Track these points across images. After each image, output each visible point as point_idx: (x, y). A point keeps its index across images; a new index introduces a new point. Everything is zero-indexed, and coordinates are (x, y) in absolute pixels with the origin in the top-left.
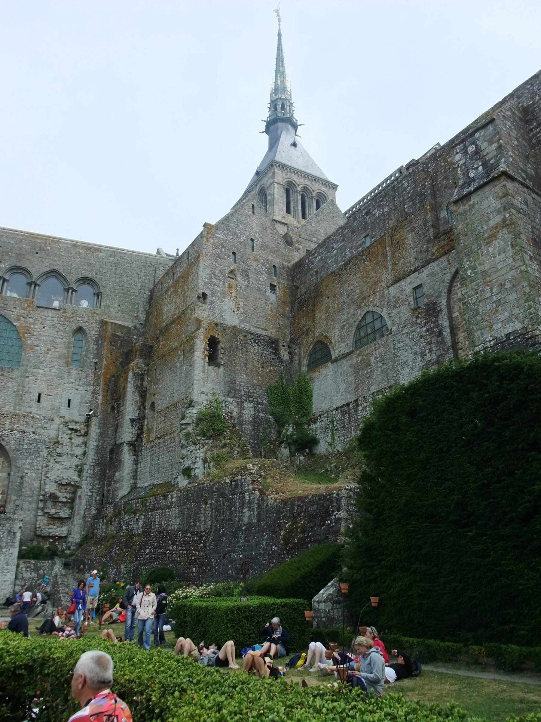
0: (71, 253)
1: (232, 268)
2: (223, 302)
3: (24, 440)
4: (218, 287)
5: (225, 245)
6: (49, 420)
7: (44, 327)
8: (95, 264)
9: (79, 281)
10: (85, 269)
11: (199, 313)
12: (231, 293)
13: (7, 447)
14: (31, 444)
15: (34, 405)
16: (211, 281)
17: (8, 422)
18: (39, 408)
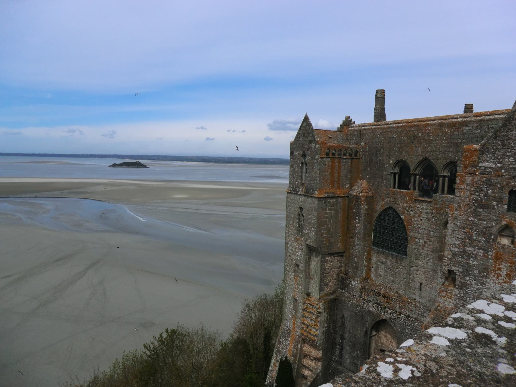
0: (439, 135)
1: (504, 223)
2: (482, 284)
3: (406, 325)
4: (476, 259)
5: (494, 181)
6: (427, 310)
7: (421, 220)
8: (461, 143)
9: (448, 165)
10: (451, 152)
11: (442, 301)
12: (500, 269)
13: (395, 328)
14: (411, 330)
15: (417, 294)
16: (464, 251)
17: (398, 306)
18: (421, 297)
